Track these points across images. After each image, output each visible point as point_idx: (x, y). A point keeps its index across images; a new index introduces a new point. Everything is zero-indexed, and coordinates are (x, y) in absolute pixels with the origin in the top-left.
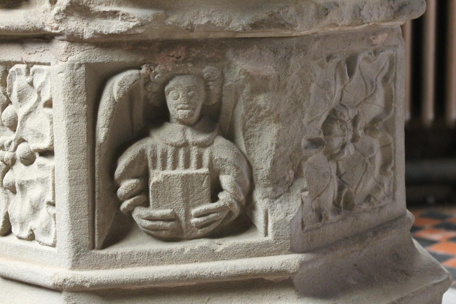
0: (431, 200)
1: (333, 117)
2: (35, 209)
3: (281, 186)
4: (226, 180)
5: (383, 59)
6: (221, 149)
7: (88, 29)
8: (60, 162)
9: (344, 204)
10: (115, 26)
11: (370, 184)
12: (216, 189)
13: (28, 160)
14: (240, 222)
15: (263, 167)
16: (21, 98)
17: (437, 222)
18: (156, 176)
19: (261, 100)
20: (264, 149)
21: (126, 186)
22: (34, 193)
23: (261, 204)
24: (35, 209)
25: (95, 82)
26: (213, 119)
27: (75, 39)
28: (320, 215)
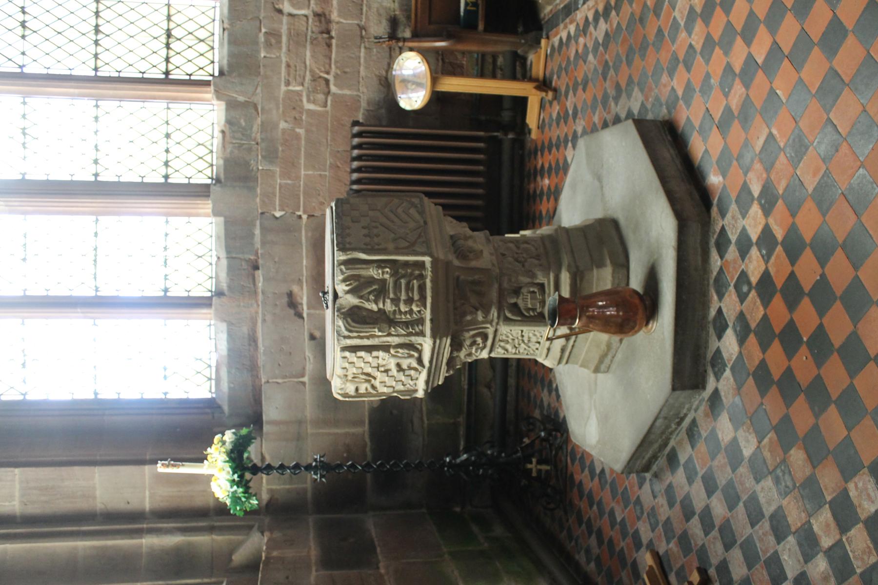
0: (521, 152)
1: (517, 260)
2: (535, 335)
3: (534, 276)
4: (532, 289)
5: (500, 243)
6: (524, 290)
7: (496, 320)
8: (525, 329)
9: (538, 257)
10: (496, 314)
11: (533, 248)
12: (534, 292)
13: (522, 336)
14: (542, 286)
15: (528, 280)
16: (508, 337)
17: (533, 156)
18: (530, 306)
19: (513, 280)
20: (525, 280)
21: (532, 314)
22: (531, 335)
23: (538, 281)
24: (535, 335)
25: (507, 320)
26: (517, 292)
27: (498, 324)
28: (541, 265)
